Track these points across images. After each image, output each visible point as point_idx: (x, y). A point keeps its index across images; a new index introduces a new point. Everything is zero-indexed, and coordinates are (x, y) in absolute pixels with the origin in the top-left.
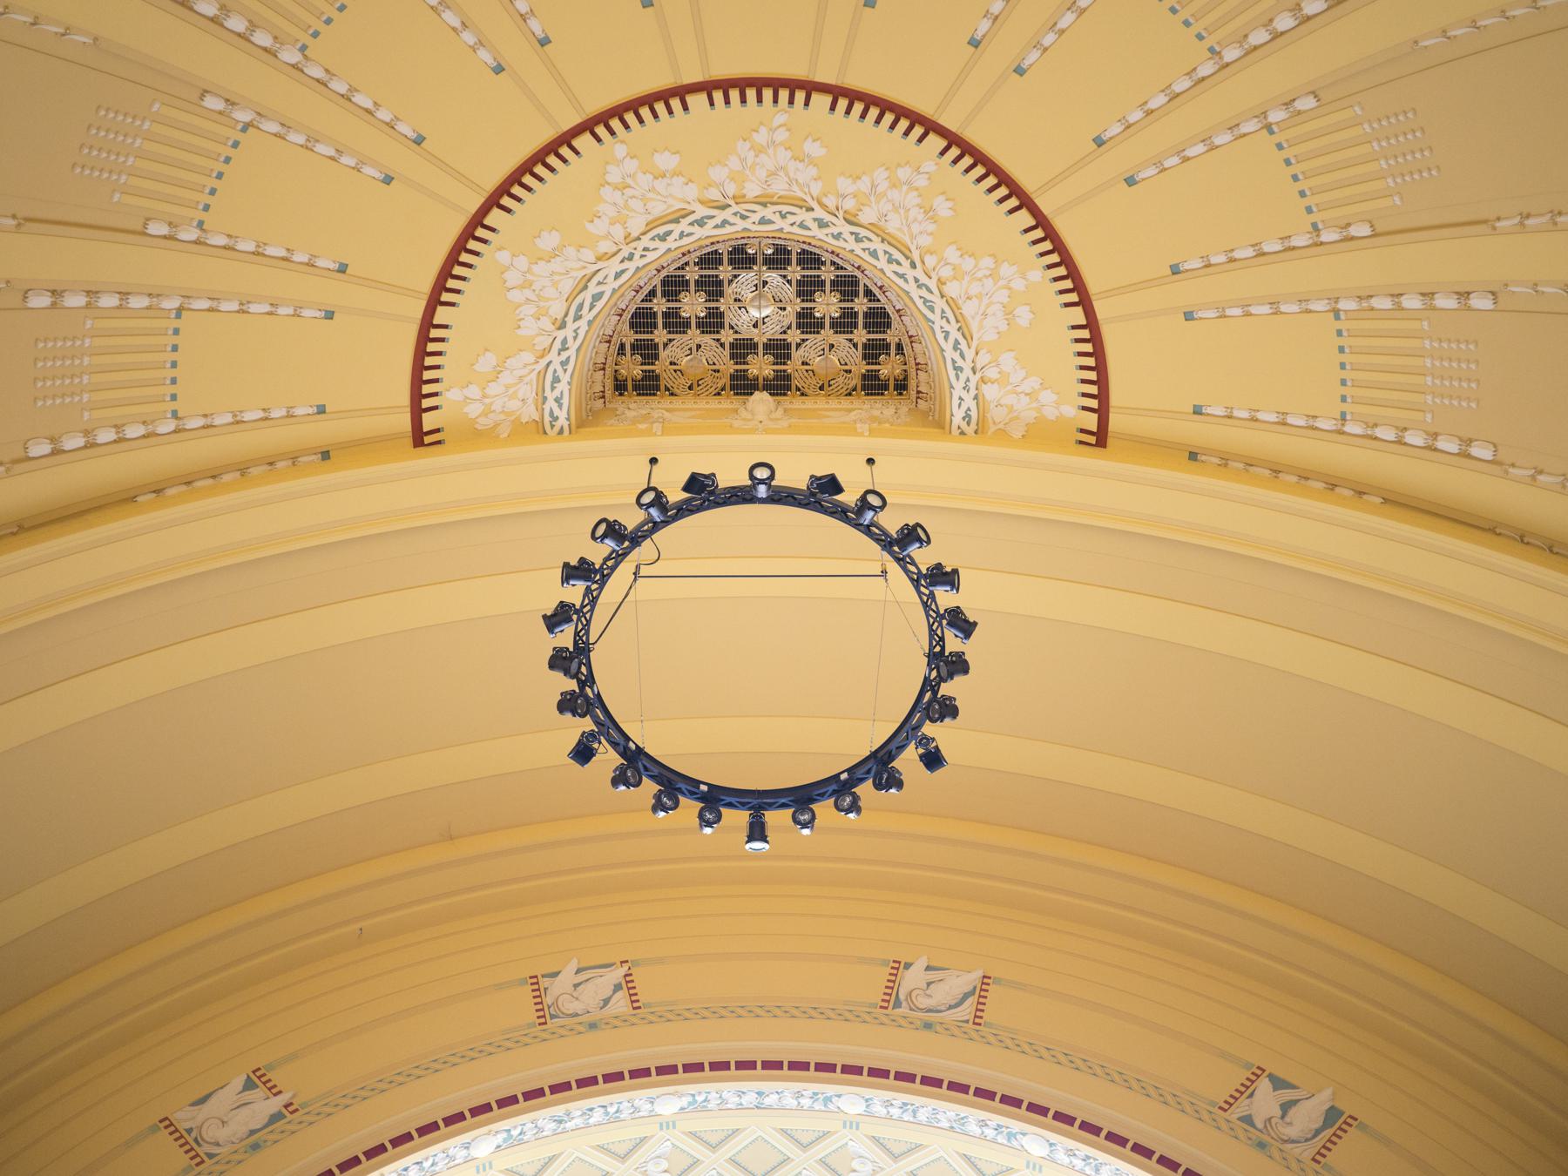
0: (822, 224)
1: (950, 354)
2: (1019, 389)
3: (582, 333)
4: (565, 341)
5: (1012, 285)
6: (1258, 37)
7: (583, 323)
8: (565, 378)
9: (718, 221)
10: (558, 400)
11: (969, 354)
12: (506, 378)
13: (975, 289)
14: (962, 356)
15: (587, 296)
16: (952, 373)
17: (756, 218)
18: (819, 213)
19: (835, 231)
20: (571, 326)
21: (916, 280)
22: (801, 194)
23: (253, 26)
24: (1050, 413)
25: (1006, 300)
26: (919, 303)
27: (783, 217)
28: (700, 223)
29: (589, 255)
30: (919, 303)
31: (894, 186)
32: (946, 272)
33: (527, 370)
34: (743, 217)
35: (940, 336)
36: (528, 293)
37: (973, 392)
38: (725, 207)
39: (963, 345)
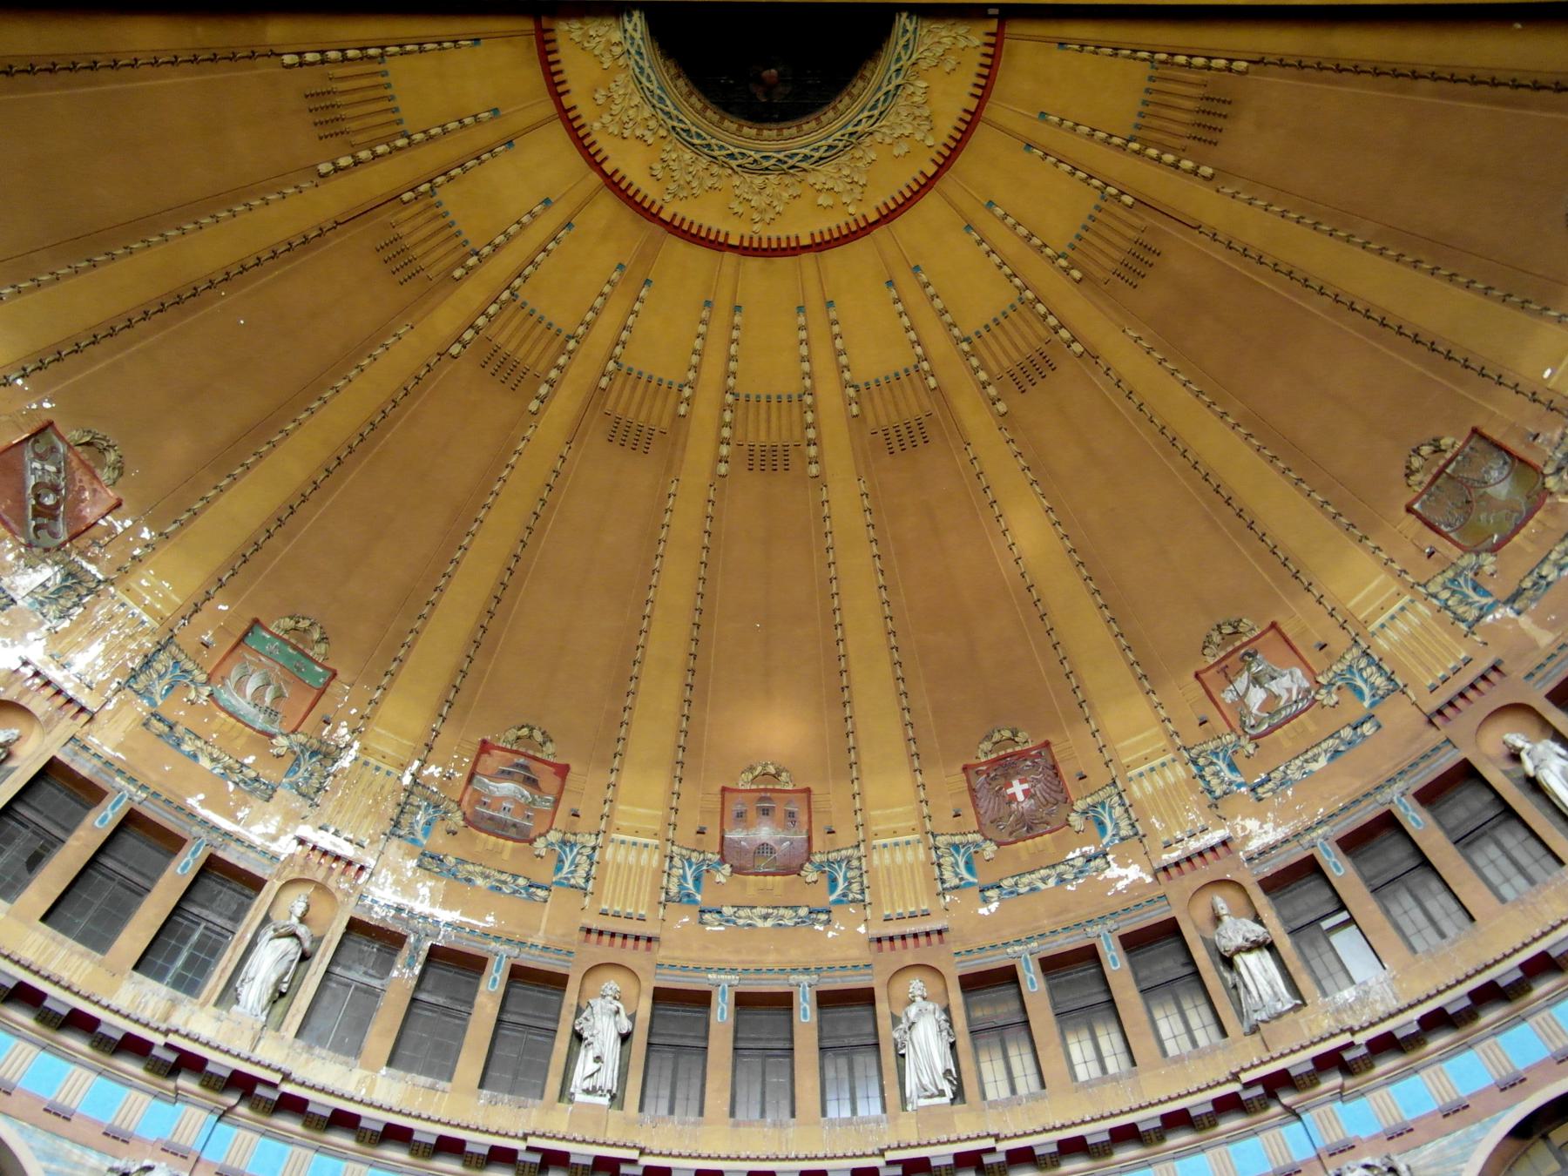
0: (731, 156)
1: (646, 65)
2: (597, 39)
3: (885, 82)
4: (897, 76)
5: (610, 118)
6: (492, 309)
7: (884, 89)
8: (899, 48)
9: (796, 159)
10: (906, 31)
11: (632, 63)
12: (939, 50)
13: (631, 112)
14: (637, 62)
15: (880, 107)
16: (643, 50)
17: (773, 161)
18: (734, 163)
19: (724, 152)
20: (891, 87)
21: (671, 118)
22: (746, 175)
23: (1045, 317)
24: (576, 25)
25: (614, 107)
26: (668, 102)
27: (755, 161)
28: (806, 157)
29: (878, 137)
30: (668, 102)
31: (689, 183)
32: (653, 124)
33: (925, 54)
34: (779, 160)
35: (653, 78)
36: (917, 112)
37: (628, 35)
38: (793, 167)
39: (637, 70)
